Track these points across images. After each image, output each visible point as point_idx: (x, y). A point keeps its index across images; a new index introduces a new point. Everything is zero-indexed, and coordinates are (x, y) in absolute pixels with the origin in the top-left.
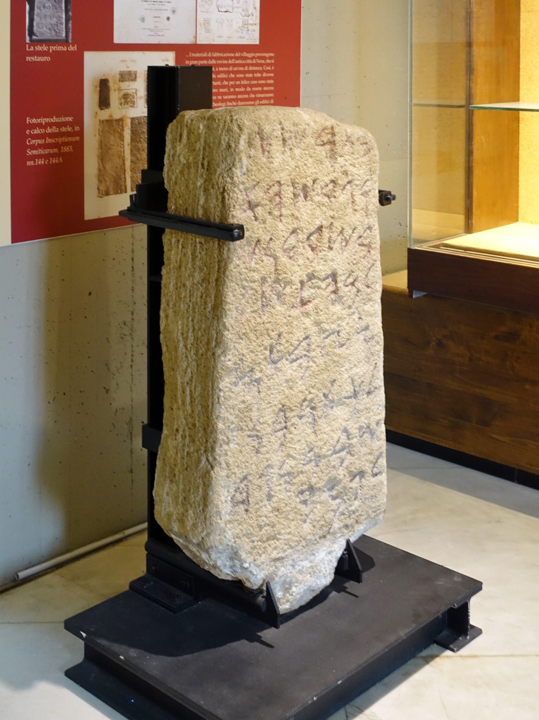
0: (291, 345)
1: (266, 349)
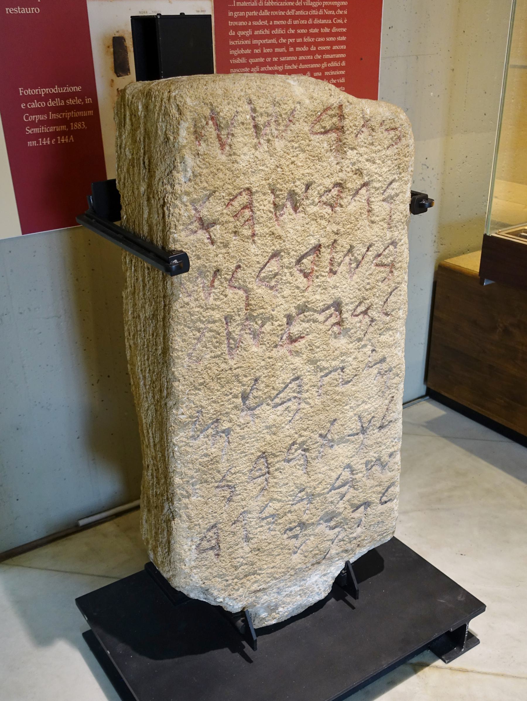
0: (273, 388)
1: (236, 397)
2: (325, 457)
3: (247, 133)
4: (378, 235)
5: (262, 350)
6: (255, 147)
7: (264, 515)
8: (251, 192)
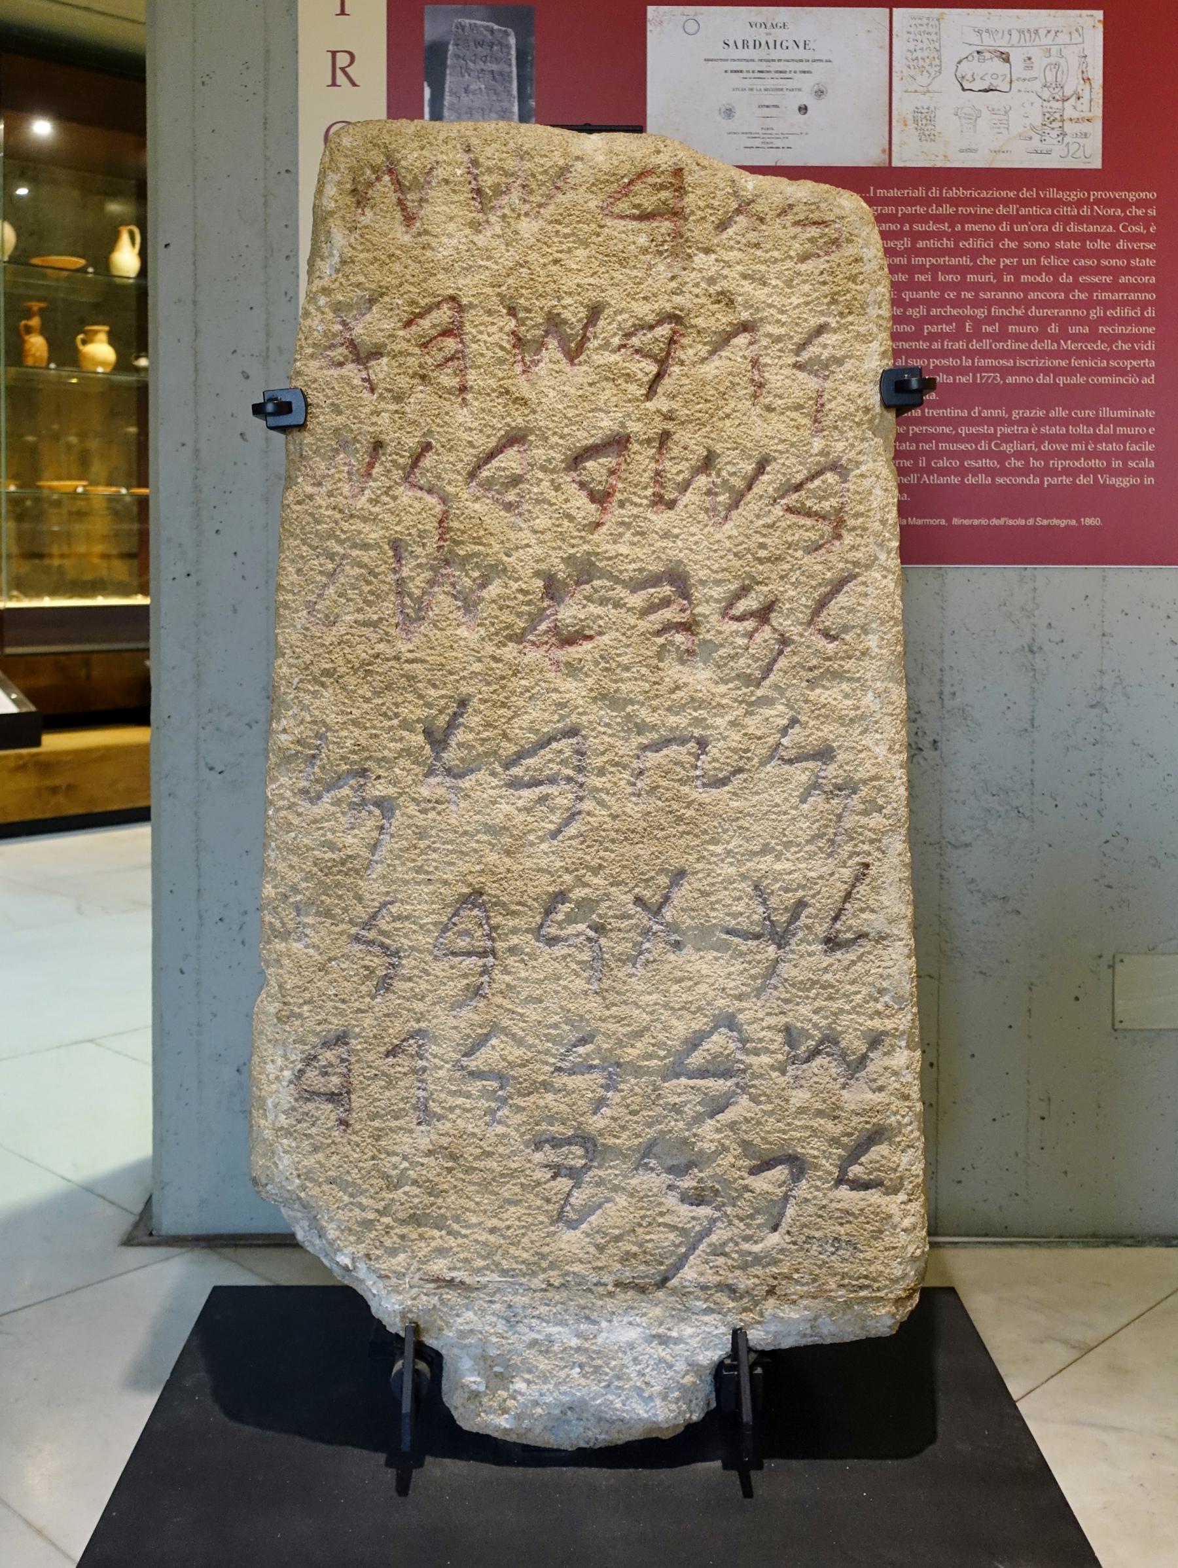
0: (505, 735)
1: (406, 725)
2: (655, 966)
3: (456, 198)
4: (783, 437)
5: (477, 636)
6: (476, 226)
7: (475, 1063)
8: (460, 306)
